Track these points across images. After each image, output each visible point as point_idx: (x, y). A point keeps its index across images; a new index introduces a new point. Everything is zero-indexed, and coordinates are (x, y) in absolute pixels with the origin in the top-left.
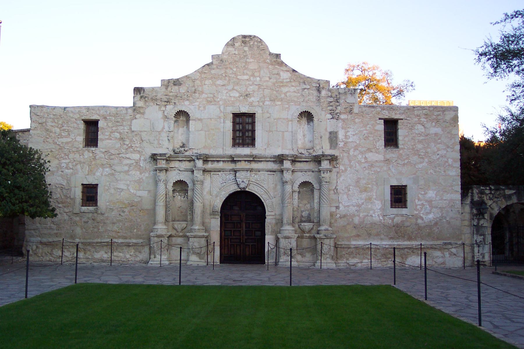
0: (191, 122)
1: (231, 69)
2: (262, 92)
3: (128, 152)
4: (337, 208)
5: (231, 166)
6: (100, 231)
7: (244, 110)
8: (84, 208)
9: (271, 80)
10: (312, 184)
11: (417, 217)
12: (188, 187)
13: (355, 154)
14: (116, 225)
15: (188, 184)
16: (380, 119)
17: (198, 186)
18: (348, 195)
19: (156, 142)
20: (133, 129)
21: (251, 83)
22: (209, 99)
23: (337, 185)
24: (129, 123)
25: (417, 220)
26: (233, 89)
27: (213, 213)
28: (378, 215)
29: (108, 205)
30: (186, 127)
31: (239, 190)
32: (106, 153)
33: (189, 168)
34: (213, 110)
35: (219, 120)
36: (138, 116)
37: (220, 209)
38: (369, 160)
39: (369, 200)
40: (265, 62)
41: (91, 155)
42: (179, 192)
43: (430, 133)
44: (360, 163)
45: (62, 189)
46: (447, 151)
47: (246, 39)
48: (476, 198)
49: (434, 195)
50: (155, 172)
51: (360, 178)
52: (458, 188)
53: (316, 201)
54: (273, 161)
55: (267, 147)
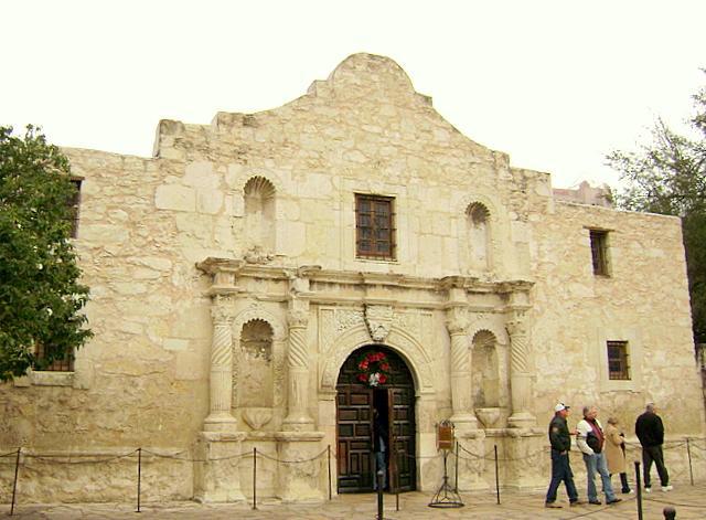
0: (278, 204)
1: (349, 109)
2: (404, 160)
3: (144, 253)
4: (534, 379)
5: (357, 295)
6: (77, 428)
7: (378, 190)
9: (418, 141)
12: (272, 334)
13: (554, 284)
14: (116, 415)
15: (271, 329)
16: (585, 227)
17: (298, 333)
18: (548, 356)
19: (207, 236)
21: (385, 140)
24: (150, 192)
27: (322, 389)
28: (593, 393)
29: (99, 369)
30: (260, 212)
31: (372, 343)
32: (96, 252)
33: (278, 294)
34: (316, 180)
35: (330, 203)
37: (336, 381)
38: (574, 296)
40: (405, 106)
43: (652, 255)
44: (562, 300)
47: (375, 62)
50: (207, 301)
51: (562, 327)
53: (502, 366)
54: (429, 290)
55: (419, 263)
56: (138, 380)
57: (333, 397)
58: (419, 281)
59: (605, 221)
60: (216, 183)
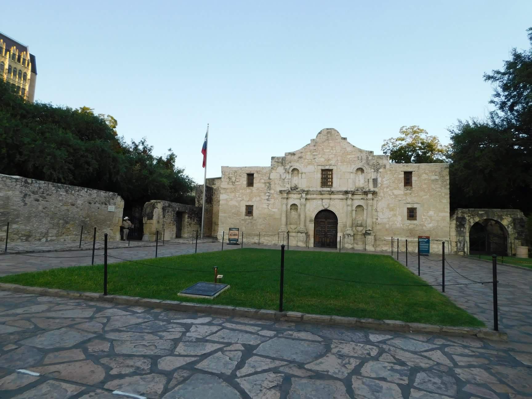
1: (320, 146)
4: (377, 219)
5: (321, 197)
7: (327, 168)
8: (247, 217)
9: (342, 152)
10: (362, 206)
11: (423, 225)
18: (383, 213)
19: (282, 184)
20: (271, 178)
21: (331, 153)
22: (309, 162)
23: (377, 207)
25: (422, 227)
26: (321, 157)
27: (311, 221)
28: (400, 224)
34: (311, 168)
36: (273, 171)
39: (395, 215)
41: (250, 191)
42: (293, 210)
45: (236, 207)
46: (441, 189)
48: (460, 215)
49: (433, 214)
52: (448, 210)
53: (365, 215)
56: (267, 218)
57: (313, 223)
58: (338, 192)
59: (411, 168)
60: (284, 171)
